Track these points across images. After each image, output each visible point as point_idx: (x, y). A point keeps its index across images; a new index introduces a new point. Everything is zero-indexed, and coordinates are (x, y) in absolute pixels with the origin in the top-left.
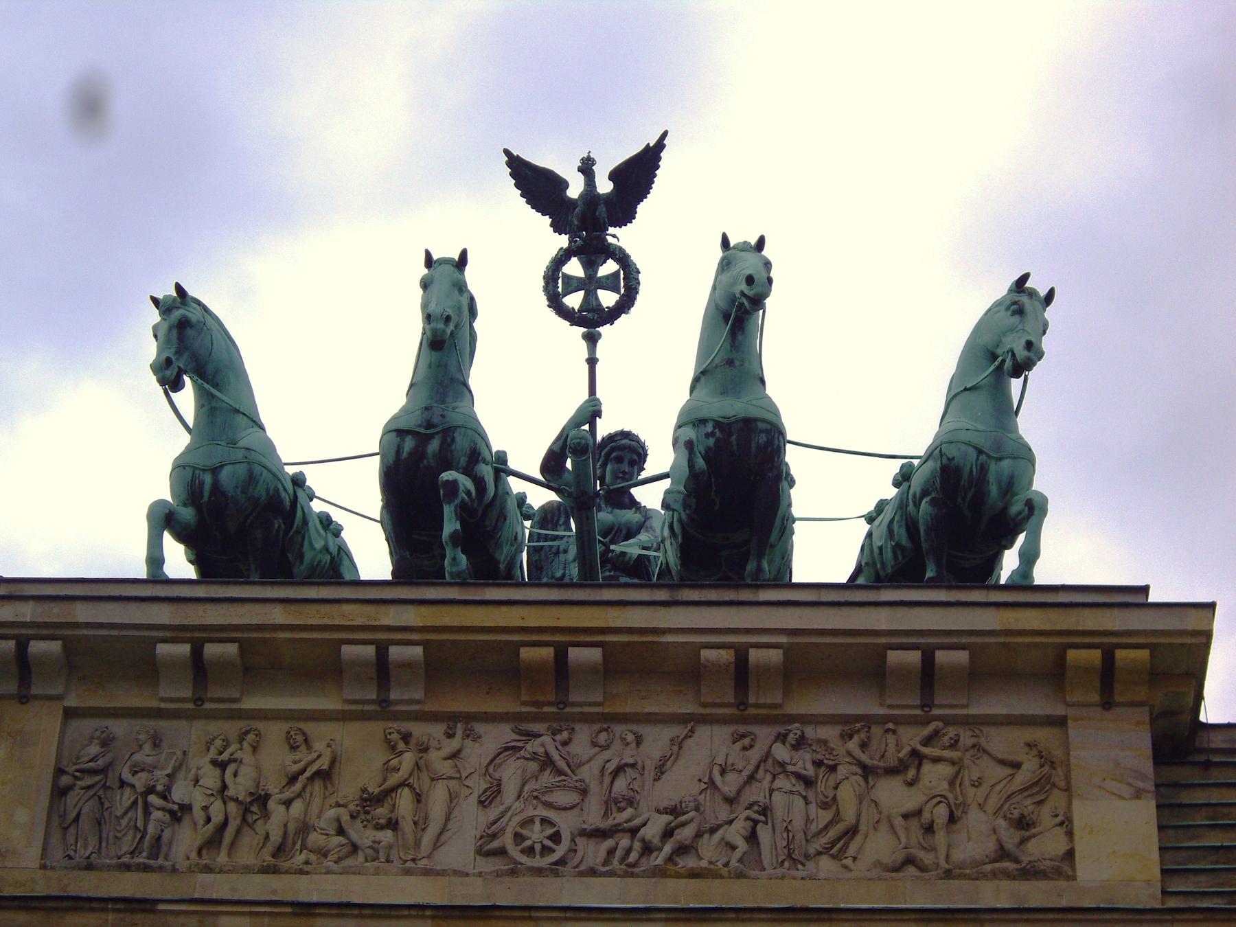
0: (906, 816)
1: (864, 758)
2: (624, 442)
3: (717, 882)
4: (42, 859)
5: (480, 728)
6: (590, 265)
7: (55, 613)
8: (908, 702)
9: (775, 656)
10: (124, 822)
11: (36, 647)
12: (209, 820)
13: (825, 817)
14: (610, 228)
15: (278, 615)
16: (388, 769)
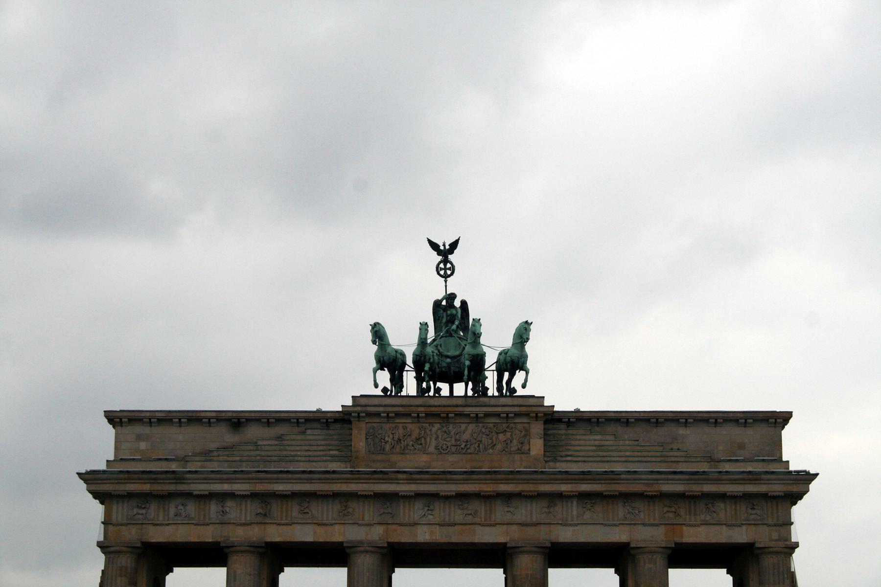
0: (503, 441)
1: (497, 431)
2: (453, 296)
3: (473, 455)
4: (365, 451)
5: (434, 425)
6: (445, 265)
7: (364, 409)
8: (505, 421)
9: (482, 415)
10: (378, 444)
11: (362, 415)
12: (392, 444)
13: (491, 441)
14: (449, 256)
15: (401, 409)
16: (420, 434)
